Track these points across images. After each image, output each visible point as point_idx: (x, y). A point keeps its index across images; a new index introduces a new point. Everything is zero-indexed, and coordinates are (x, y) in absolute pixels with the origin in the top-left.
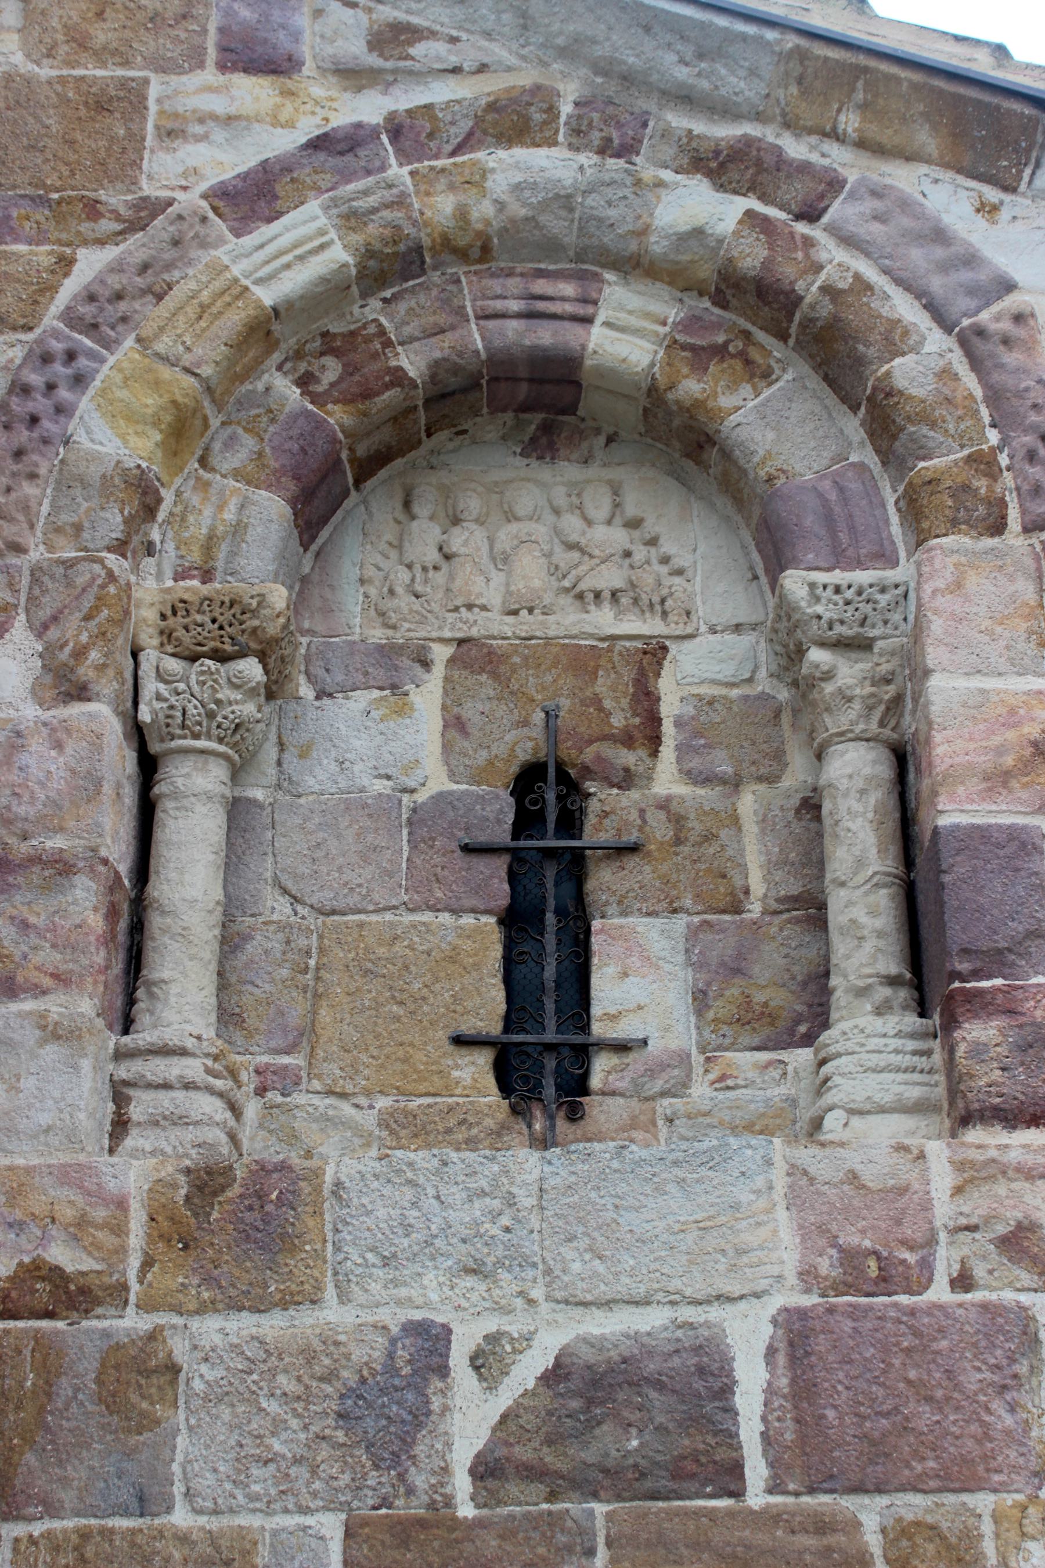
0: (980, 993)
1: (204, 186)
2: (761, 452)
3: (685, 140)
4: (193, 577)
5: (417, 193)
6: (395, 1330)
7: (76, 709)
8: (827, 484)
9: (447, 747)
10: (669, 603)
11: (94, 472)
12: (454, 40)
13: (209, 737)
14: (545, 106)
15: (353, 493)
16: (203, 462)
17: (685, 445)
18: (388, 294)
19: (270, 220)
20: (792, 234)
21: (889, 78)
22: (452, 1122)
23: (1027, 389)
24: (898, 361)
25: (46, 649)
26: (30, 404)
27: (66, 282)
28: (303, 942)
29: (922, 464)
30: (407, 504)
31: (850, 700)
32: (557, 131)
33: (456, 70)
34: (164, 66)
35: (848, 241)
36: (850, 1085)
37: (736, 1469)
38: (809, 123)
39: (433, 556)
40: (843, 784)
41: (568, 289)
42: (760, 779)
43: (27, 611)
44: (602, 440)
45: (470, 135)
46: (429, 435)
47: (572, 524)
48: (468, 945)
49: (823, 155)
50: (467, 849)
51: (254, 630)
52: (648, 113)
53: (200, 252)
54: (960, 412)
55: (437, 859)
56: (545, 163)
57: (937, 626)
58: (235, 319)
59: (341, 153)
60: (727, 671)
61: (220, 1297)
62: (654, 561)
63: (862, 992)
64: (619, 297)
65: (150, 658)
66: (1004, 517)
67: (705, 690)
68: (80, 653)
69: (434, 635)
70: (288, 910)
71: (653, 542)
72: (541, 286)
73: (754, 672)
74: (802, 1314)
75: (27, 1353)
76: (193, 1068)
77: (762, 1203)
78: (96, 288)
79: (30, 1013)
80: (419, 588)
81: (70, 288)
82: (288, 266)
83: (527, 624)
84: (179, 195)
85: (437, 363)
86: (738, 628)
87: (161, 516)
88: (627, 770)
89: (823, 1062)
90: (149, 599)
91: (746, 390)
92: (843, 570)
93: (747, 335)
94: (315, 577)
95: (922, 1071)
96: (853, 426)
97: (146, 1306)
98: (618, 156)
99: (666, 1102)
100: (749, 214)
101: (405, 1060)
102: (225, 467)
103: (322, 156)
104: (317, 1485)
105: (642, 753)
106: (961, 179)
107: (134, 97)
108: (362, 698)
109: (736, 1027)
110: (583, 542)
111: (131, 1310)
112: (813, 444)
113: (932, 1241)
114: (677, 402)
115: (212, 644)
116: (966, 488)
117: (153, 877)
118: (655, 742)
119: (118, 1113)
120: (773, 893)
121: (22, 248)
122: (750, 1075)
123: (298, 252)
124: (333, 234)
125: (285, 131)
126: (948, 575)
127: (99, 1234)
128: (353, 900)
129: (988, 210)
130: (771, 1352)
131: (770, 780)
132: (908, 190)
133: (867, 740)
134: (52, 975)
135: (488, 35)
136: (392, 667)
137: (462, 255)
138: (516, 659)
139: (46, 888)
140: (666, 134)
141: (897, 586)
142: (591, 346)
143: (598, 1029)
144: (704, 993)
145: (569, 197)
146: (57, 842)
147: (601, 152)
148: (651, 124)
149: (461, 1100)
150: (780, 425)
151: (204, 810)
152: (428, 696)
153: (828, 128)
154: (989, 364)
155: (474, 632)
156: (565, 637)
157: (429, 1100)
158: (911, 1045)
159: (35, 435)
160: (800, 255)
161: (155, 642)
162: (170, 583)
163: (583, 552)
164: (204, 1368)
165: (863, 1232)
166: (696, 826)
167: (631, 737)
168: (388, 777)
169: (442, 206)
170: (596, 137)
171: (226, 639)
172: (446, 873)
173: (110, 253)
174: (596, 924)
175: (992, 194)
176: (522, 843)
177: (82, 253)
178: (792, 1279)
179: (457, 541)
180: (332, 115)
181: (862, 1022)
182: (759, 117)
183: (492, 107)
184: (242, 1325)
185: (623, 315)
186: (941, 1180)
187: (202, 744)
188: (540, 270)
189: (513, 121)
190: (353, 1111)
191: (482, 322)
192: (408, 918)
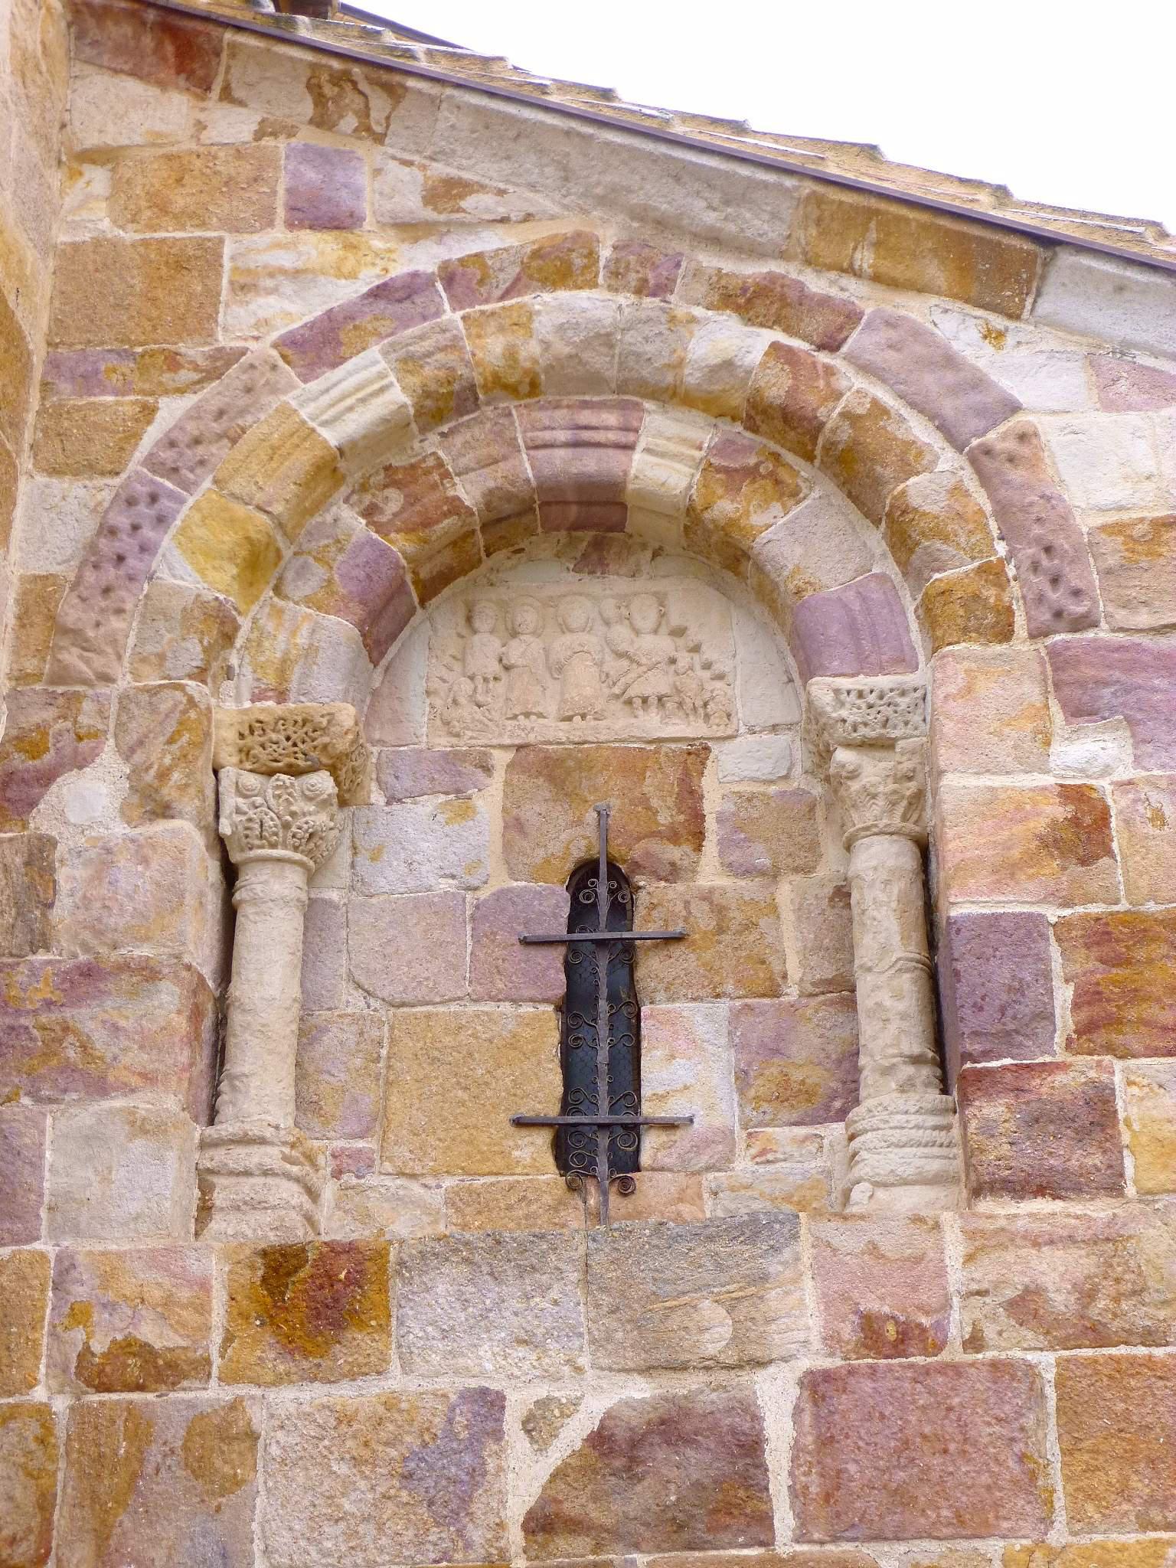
0: (989, 1072)
1: (274, 336)
2: (791, 567)
3: (715, 279)
4: (270, 698)
5: (469, 336)
6: (453, 1398)
7: (161, 826)
8: (851, 595)
9: (507, 846)
10: (711, 706)
11: (176, 605)
12: (501, 192)
13: (285, 847)
14: (585, 252)
15: (419, 610)
16: (277, 590)
17: (724, 559)
18: (445, 429)
19: (334, 365)
20: (814, 364)
21: (899, 219)
22: (513, 1200)
23: (1031, 504)
24: (913, 480)
25: (133, 771)
26: (117, 544)
27: (150, 429)
28: (375, 1033)
29: (937, 576)
30: (469, 620)
31: (874, 796)
32: (596, 276)
33: (504, 220)
34: (236, 227)
35: (866, 369)
36: (876, 1161)
37: (765, 1520)
38: (828, 261)
39: (495, 668)
40: (869, 876)
41: (611, 418)
42: (796, 870)
43: (116, 736)
44: (649, 554)
45: (518, 279)
46: (488, 556)
47: (621, 633)
48: (527, 1033)
49: (842, 289)
50: (526, 942)
51: (325, 747)
52: (681, 254)
53: (271, 398)
54: (971, 526)
55: (498, 952)
56: (586, 304)
57: (949, 728)
58: (302, 461)
59: (400, 301)
60: (765, 769)
61: (294, 1370)
62: (698, 667)
63: (887, 1071)
64: (658, 425)
65: (229, 774)
66: (1011, 625)
67: (747, 788)
68: (163, 775)
69: (495, 742)
70: (362, 1004)
71: (696, 649)
72: (586, 417)
73: (790, 769)
74: (827, 1376)
75: (120, 1423)
76: (270, 1156)
77: (789, 1274)
78: (175, 435)
79: (121, 1110)
80: (480, 698)
82: (351, 409)
83: (580, 729)
84: (252, 345)
85: (491, 492)
86: (774, 728)
87: (239, 642)
88: (673, 864)
89: (852, 1138)
90: (228, 720)
91: (776, 508)
92: (867, 675)
93: (776, 457)
94: (385, 691)
95: (941, 1146)
96: (875, 539)
97: (230, 1377)
98: (654, 295)
99: (711, 1176)
100: (775, 347)
101: (470, 1142)
102: (298, 595)
103: (382, 304)
104: (384, 1541)
105: (687, 848)
106: (969, 309)
107: (209, 256)
108: (429, 804)
109: (775, 1104)
110: (632, 651)
111: (213, 1382)
112: (838, 557)
113: (946, 1305)
114: (713, 521)
115: (287, 760)
116: (976, 597)
117: (234, 978)
118: (698, 837)
119: (202, 1199)
120: (809, 978)
121: (110, 399)
122: (788, 1149)
123: (360, 395)
124: (392, 378)
125: (348, 282)
126: (960, 681)
127: (184, 1313)
128: (421, 993)
129: (994, 336)
130: (797, 1411)
131: (806, 870)
132: (920, 320)
133: (891, 834)
134: (140, 1074)
135: (532, 187)
136: (456, 774)
137: (513, 390)
138: (571, 763)
139: (134, 993)
140: (697, 273)
141: (915, 690)
142: (633, 472)
143: (647, 1109)
144: (746, 1073)
145: (608, 335)
146: (144, 951)
147: (638, 292)
148: (684, 264)
149: (521, 1178)
150: (805, 537)
151: (281, 914)
152: (489, 800)
153: (845, 265)
154: (996, 481)
155: (531, 738)
156: (615, 741)
157: (493, 1179)
158: (932, 1120)
159: (121, 573)
160: (821, 383)
161: (235, 759)
162: (247, 704)
163: (632, 661)
164: (280, 1435)
165: (882, 1298)
166: (736, 917)
167: (676, 834)
168: (453, 877)
169: (493, 348)
170: (633, 278)
171: (300, 755)
172: (506, 965)
173: (190, 400)
174: (645, 1010)
175: (998, 322)
176: (576, 936)
177: (164, 402)
178: (817, 1344)
179: (515, 652)
180: (391, 266)
181: (885, 1099)
182: (783, 256)
183: (536, 254)
184: (314, 1394)
185: (661, 442)
186: (954, 1247)
187: (278, 852)
188: (585, 402)
189: (555, 266)
190: (422, 1191)
191: (532, 452)
192: (472, 1008)
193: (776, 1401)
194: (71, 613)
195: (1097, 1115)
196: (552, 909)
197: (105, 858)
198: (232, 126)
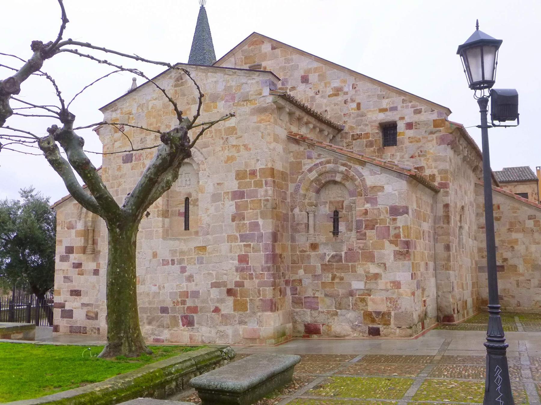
58: (309, 182)
64: (338, 175)
81: (298, 179)
107: (301, 161)
129: (362, 169)
152: (328, 205)
189: (328, 162)
193: (343, 254)
194: (294, 196)
195: (365, 234)
196: (332, 216)
197: (298, 215)
198: (302, 149)
